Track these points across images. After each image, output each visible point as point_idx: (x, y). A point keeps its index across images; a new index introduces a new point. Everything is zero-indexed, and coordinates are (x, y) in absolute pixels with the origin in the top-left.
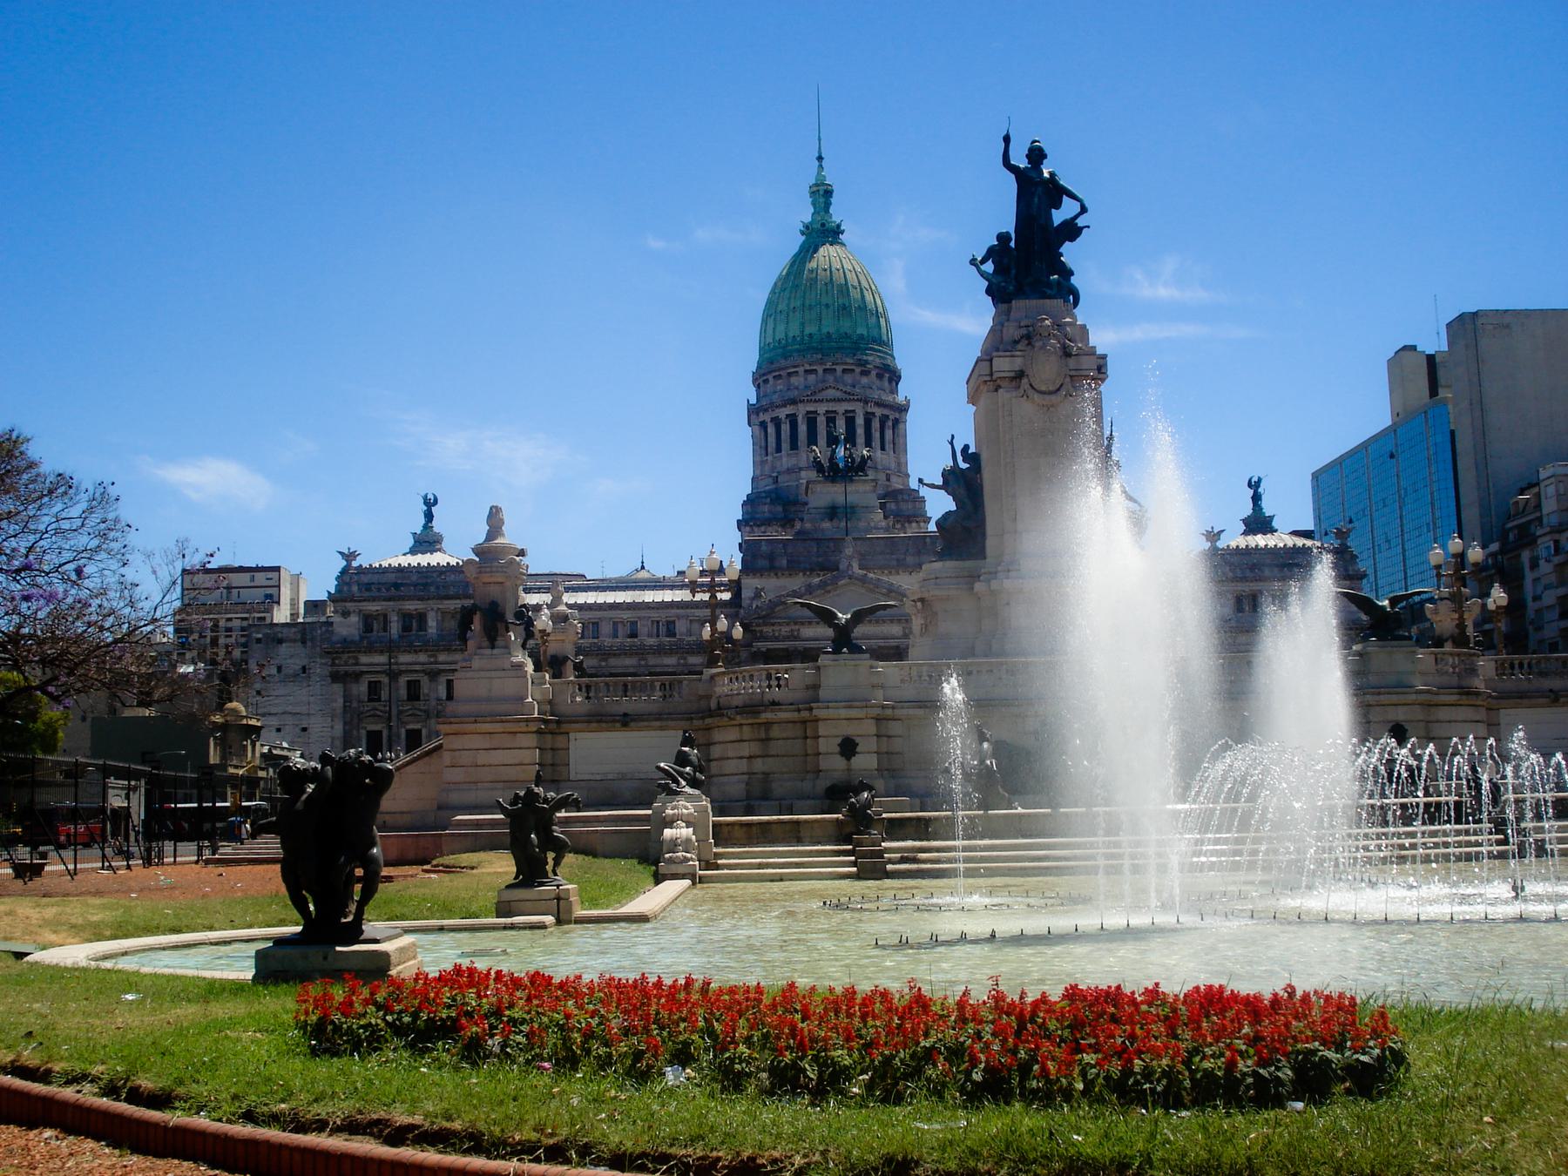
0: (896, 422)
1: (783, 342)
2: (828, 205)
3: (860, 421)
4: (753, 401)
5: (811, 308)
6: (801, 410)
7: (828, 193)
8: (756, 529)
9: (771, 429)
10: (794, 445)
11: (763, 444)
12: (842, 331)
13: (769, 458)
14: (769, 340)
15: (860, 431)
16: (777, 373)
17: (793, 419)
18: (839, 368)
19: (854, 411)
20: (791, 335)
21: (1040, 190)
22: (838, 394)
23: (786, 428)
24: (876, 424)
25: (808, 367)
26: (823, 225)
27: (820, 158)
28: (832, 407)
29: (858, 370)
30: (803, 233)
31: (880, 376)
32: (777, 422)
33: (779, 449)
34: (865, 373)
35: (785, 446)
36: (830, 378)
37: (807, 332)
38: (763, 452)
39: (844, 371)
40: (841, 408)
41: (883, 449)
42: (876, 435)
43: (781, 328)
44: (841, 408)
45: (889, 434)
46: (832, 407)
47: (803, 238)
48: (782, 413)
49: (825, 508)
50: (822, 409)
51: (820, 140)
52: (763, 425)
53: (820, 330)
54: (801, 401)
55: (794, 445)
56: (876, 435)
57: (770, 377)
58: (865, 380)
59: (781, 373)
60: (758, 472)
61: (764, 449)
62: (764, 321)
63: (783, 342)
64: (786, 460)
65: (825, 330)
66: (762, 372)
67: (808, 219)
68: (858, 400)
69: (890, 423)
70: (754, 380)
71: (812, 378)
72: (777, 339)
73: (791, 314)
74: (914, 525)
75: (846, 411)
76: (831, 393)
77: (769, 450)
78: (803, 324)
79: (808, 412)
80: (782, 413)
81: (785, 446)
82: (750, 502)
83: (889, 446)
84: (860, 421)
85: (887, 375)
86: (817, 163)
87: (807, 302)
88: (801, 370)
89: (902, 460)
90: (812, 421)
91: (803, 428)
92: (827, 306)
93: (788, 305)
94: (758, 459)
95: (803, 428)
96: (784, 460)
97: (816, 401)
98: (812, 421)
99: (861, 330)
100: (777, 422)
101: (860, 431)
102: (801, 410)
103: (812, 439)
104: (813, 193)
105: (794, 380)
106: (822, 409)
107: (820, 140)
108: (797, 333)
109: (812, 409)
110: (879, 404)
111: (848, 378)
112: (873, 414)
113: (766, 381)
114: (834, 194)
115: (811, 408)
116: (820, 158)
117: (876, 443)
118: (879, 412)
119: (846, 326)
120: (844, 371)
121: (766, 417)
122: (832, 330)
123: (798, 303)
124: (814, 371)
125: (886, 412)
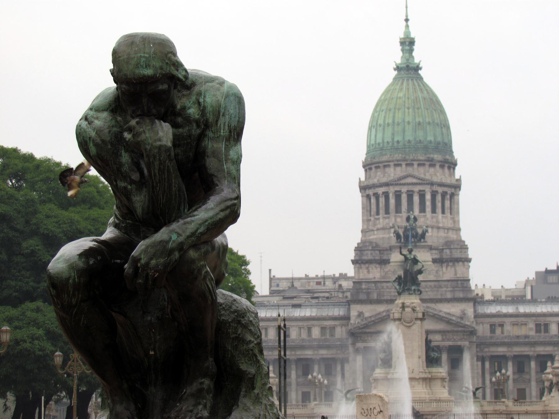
0: (452, 195)
1: (381, 145)
2: (411, 51)
3: (428, 197)
4: (363, 179)
5: (398, 124)
6: (392, 190)
7: (412, 43)
8: (363, 266)
9: (373, 200)
10: (387, 212)
11: (369, 209)
12: (418, 139)
13: (372, 219)
14: (373, 142)
15: (428, 203)
16: (377, 165)
17: (386, 195)
18: (416, 163)
19: (424, 191)
20: (386, 141)
21: (410, 262)
22: (415, 181)
23: (382, 200)
24: (439, 198)
25: (396, 163)
26: (408, 66)
27: (407, 20)
28: (410, 188)
29: (427, 163)
30: (395, 69)
31: (442, 167)
32: (377, 196)
33: (378, 213)
34: (432, 165)
35: (382, 211)
36: (410, 170)
37: (396, 139)
38: (369, 214)
39: (419, 165)
40: (416, 189)
41: (443, 212)
42: (439, 205)
43: (380, 135)
44: (416, 189)
45: (447, 203)
46: (410, 188)
47: (396, 72)
48: (380, 191)
49: (400, 262)
50: (404, 189)
51: (407, 7)
52: (368, 197)
53: (404, 138)
54: (392, 185)
55: (387, 212)
56: (439, 205)
57: (373, 166)
58: (432, 170)
59: (380, 165)
60: (365, 227)
61: (367, 210)
62: (370, 129)
63: (381, 145)
64: (382, 222)
65: (407, 139)
66: (368, 163)
67: (399, 61)
68: (427, 184)
69: (448, 197)
70: (364, 167)
71: (398, 169)
72: (377, 142)
73: (386, 127)
74: (461, 263)
75: (420, 191)
76: (410, 180)
77: (372, 213)
78: (393, 134)
79: (396, 191)
80: (380, 191)
81: (382, 211)
82: (359, 249)
83: (447, 211)
84: (428, 197)
85: (447, 165)
86: (404, 23)
87: (396, 121)
88: (392, 164)
89: (456, 219)
90: (398, 196)
91: (392, 201)
92: (409, 123)
93: (384, 121)
94: (365, 218)
95: (392, 201)
96: (381, 220)
97: (401, 184)
98: (398, 196)
99: (430, 138)
100: (377, 196)
101: (428, 203)
102: (392, 190)
103: (398, 210)
104: (402, 43)
105: (387, 169)
106: (404, 189)
107: (407, 7)
108: (390, 140)
109: (398, 189)
110: (441, 185)
111: (421, 169)
112: (437, 192)
113: (370, 169)
114: (416, 44)
115: (397, 188)
116: (407, 20)
117: (439, 210)
118: (440, 190)
119: (420, 134)
120: (419, 165)
121: (370, 192)
122: (411, 139)
123: (390, 121)
124: (400, 165)
125: (445, 189)
